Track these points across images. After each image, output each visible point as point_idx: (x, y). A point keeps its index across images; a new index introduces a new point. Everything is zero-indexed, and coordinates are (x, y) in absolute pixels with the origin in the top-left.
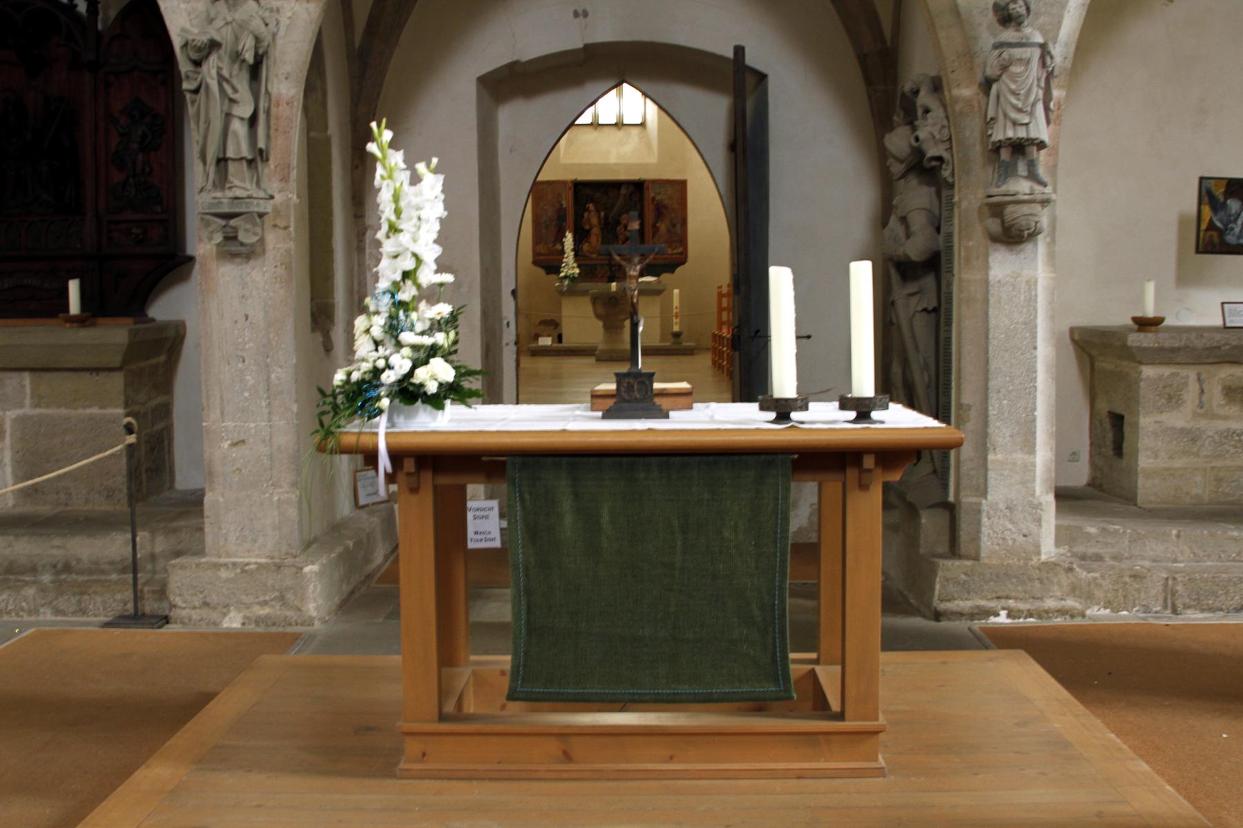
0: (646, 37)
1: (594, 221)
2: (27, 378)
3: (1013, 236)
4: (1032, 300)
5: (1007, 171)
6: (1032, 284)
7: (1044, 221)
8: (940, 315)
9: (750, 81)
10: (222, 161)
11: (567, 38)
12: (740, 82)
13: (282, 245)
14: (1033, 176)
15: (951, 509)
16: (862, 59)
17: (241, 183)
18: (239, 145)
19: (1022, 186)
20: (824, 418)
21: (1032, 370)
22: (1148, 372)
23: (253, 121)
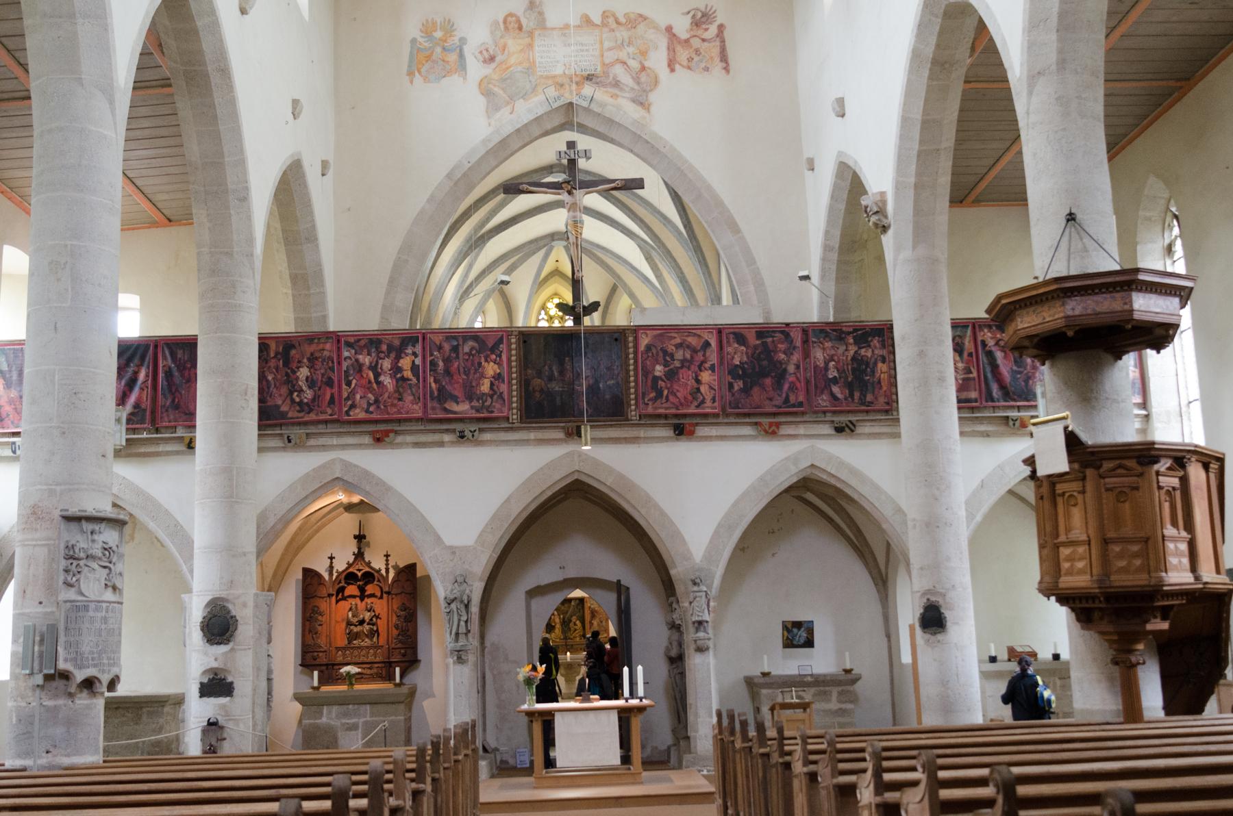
0: (586, 575)
1: (557, 620)
2: (368, 707)
3: (701, 650)
4: (709, 669)
5: (697, 630)
6: (709, 664)
7: (711, 646)
8: (682, 674)
9: (623, 590)
10: (457, 634)
11: (558, 576)
12: (620, 589)
13: (471, 658)
14: (705, 631)
15: (688, 738)
16: (663, 582)
17: (462, 641)
18: (463, 630)
19: (701, 634)
20: (634, 702)
21: (710, 692)
22: (764, 691)
23: (466, 622)
